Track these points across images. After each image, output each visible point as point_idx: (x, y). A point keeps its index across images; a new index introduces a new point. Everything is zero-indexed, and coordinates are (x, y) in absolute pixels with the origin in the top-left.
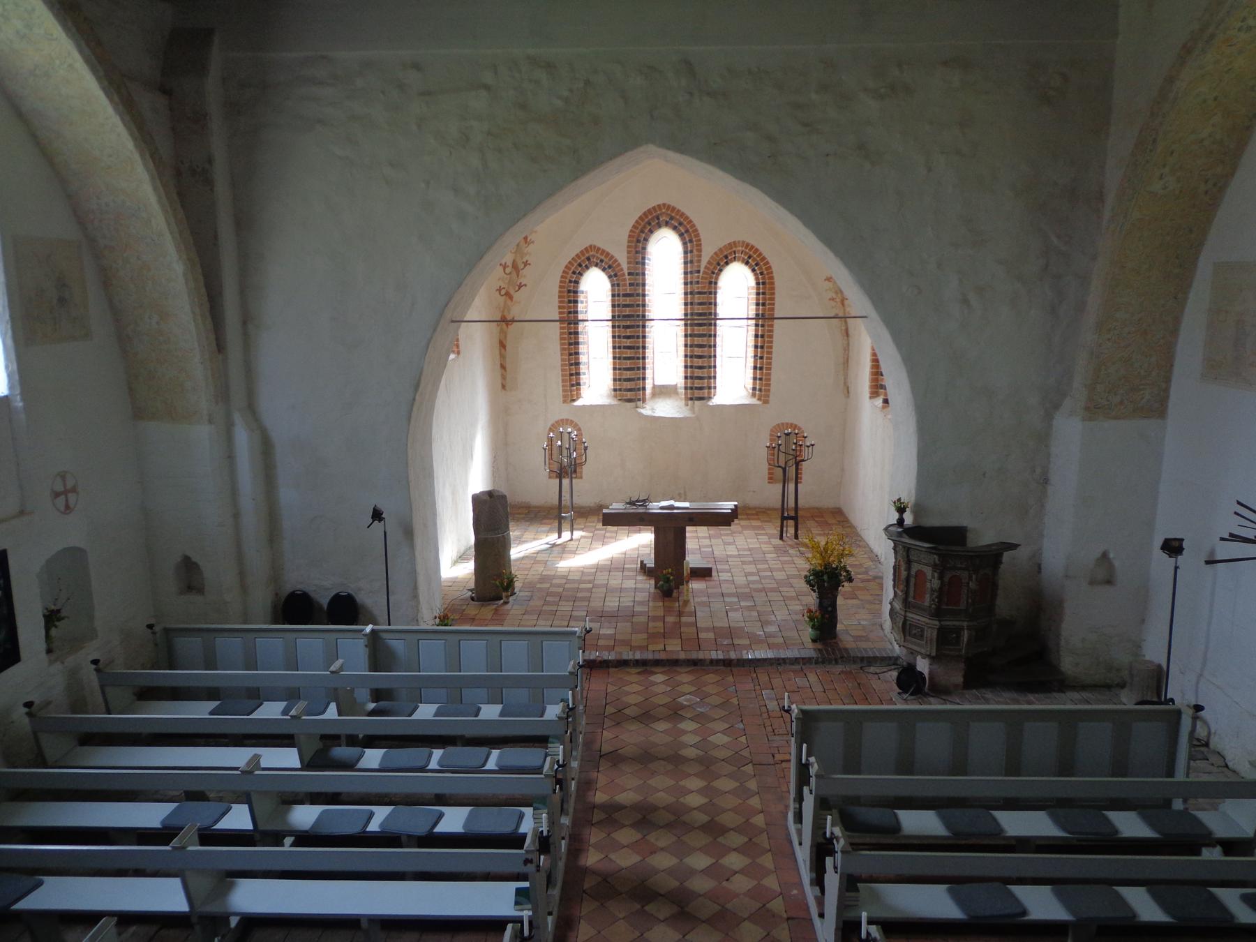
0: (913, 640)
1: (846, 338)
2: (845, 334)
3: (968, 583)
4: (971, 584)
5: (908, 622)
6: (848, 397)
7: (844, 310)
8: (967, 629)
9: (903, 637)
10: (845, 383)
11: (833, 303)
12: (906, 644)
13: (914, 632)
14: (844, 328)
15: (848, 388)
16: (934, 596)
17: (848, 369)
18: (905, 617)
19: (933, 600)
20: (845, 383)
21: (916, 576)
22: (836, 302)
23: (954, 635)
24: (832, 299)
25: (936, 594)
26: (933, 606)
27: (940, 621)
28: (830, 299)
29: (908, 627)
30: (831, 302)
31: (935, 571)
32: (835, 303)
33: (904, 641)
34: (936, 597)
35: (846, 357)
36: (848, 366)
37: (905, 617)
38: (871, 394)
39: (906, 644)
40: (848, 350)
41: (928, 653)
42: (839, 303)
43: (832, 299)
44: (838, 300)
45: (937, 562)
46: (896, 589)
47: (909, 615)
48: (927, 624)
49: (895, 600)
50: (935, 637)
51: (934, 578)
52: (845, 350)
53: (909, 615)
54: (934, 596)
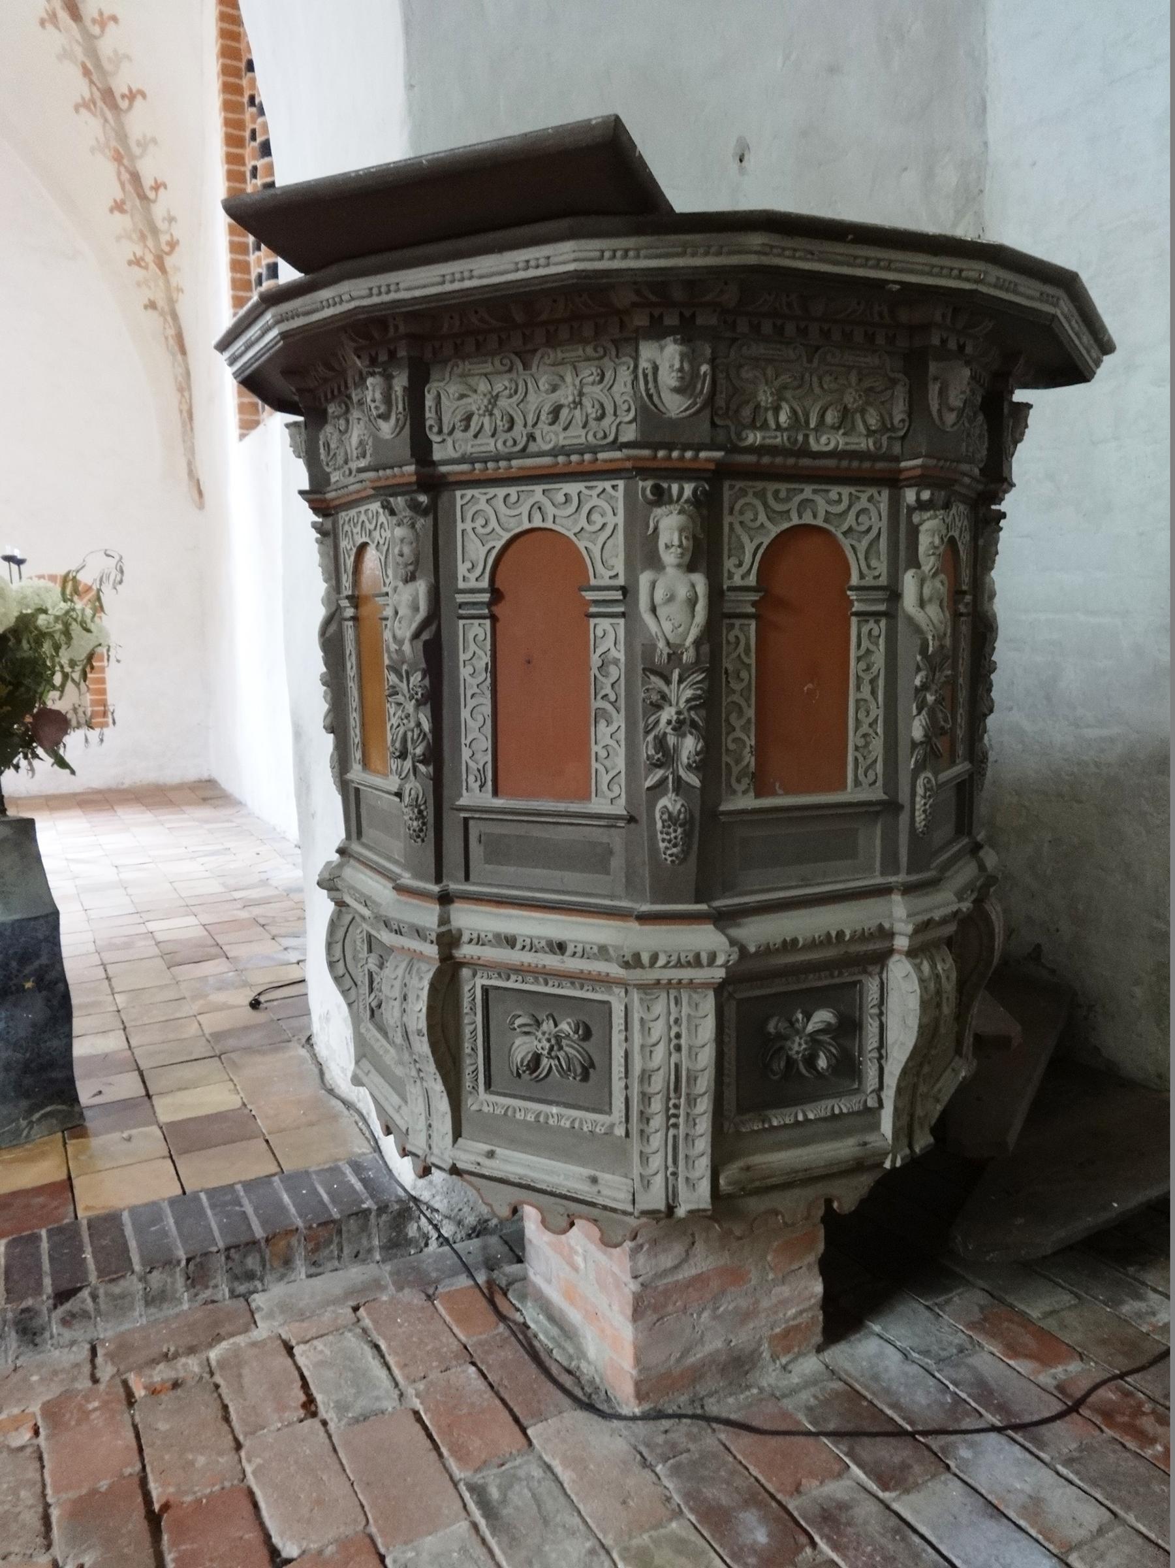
0: (528, 1110)
1: (179, 357)
2: (176, 348)
3: (894, 594)
4: (909, 583)
5: (472, 986)
6: (201, 506)
7: (167, 282)
8: (911, 954)
9: (442, 1105)
10: (191, 473)
11: (136, 270)
12: (469, 1154)
13: (522, 1048)
14: (171, 332)
15: (198, 481)
16: (668, 714)
17: (193, 437)
18: (448, 941)
19: (665, 756)
20: (191, 473)
21: (496, 595)
22: (146, 268)
23: (823, 1017)
24: (137, 262)
25: (682, 694)
26: (669, 802)
27: (722, 919)
28: (130, 263)
29: (472, 1022)
30: (136, 268)
31: (660, 497)
32: (143, 272)
33: (457, 1134)
34: (679, 727)
35: (185, 407)
36: (192, 429)
37: (448, 941)
38: (241, 427)
39: (469, 1154)
40: (189, 389)
41: (655, 1199)
42: (152, 266)
43: (137, 262)
44: (149, 258)
45: (674, 405)
46: (356, 773)
47: (467, 918)
48: (633, 962)
49: (356, 847)
50: (707, 1057)
51: (654, 562)
52: (181, 390)
53: (467, 918)
54: (668, 714)
